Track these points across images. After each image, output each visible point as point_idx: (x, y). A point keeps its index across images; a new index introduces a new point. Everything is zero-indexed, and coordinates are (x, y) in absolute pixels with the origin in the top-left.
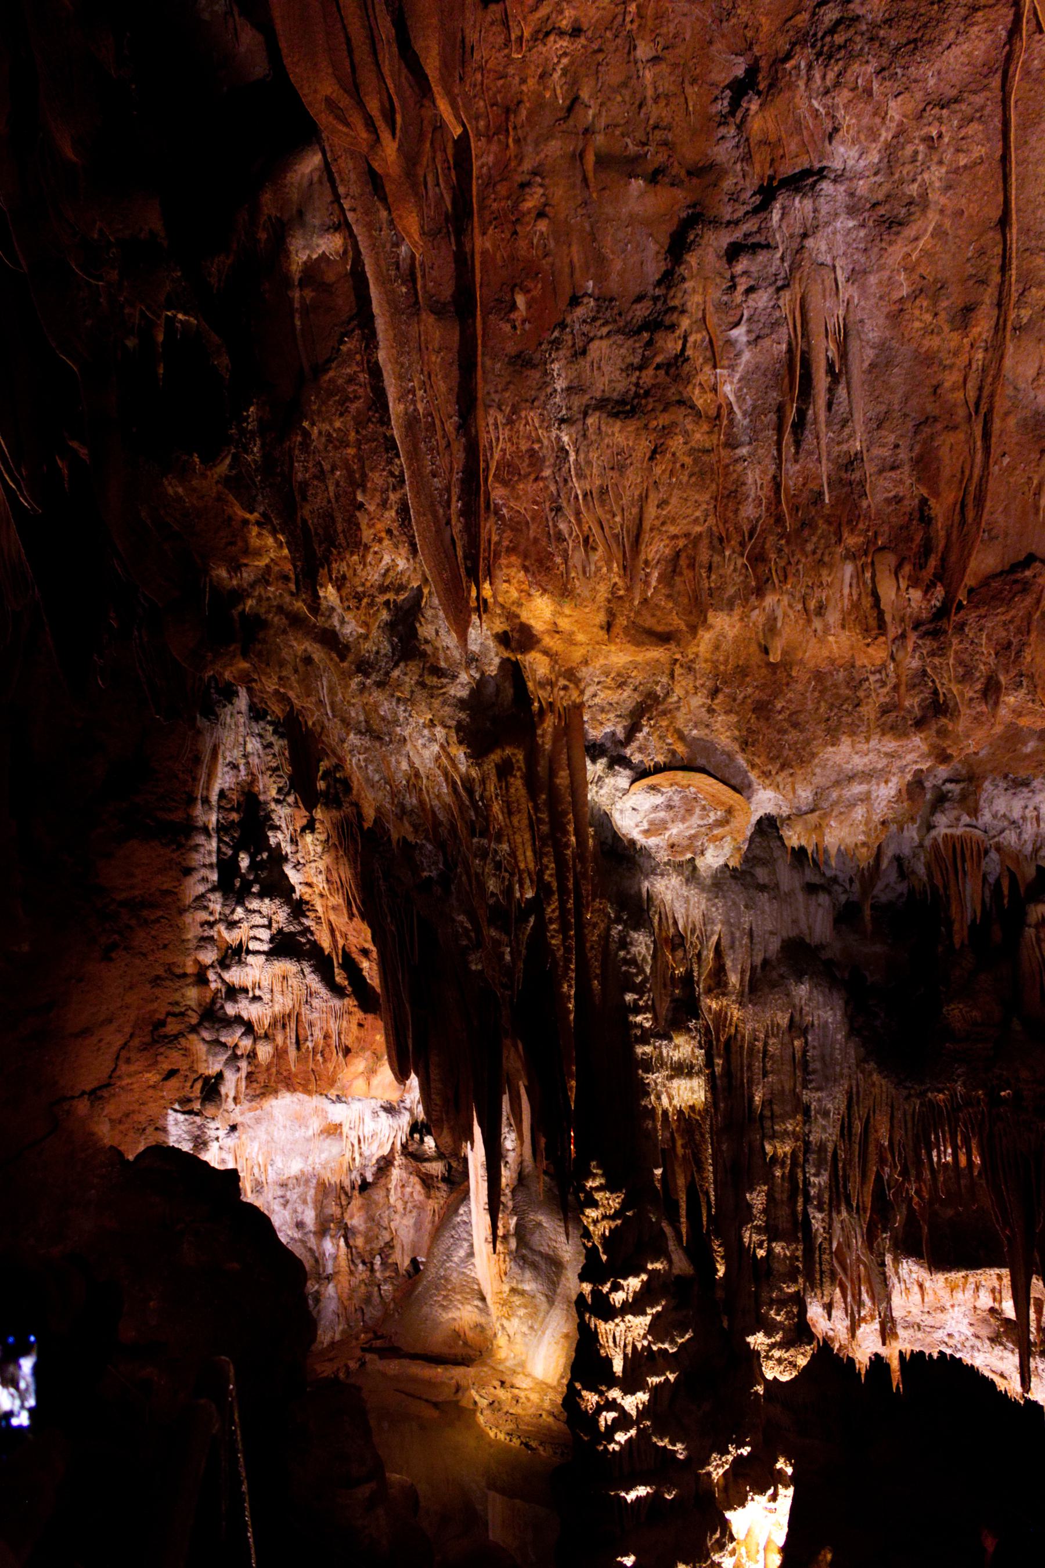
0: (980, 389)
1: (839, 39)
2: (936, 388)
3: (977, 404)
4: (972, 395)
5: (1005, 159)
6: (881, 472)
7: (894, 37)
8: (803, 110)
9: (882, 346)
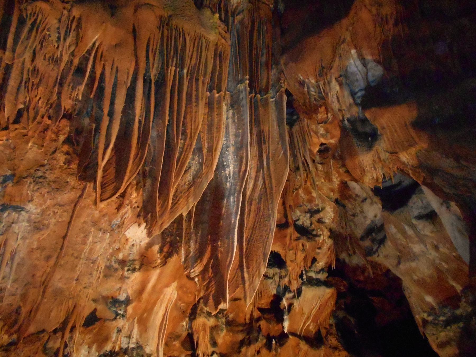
0: (46, 279)
1: (41, 180)
2: (33, 276)
3: (44, 283)
4: (43, 279)
5: (70, 223)
6: (9, 295)
7: (54, 186)
8: (24, 192)
9: (23, 259)
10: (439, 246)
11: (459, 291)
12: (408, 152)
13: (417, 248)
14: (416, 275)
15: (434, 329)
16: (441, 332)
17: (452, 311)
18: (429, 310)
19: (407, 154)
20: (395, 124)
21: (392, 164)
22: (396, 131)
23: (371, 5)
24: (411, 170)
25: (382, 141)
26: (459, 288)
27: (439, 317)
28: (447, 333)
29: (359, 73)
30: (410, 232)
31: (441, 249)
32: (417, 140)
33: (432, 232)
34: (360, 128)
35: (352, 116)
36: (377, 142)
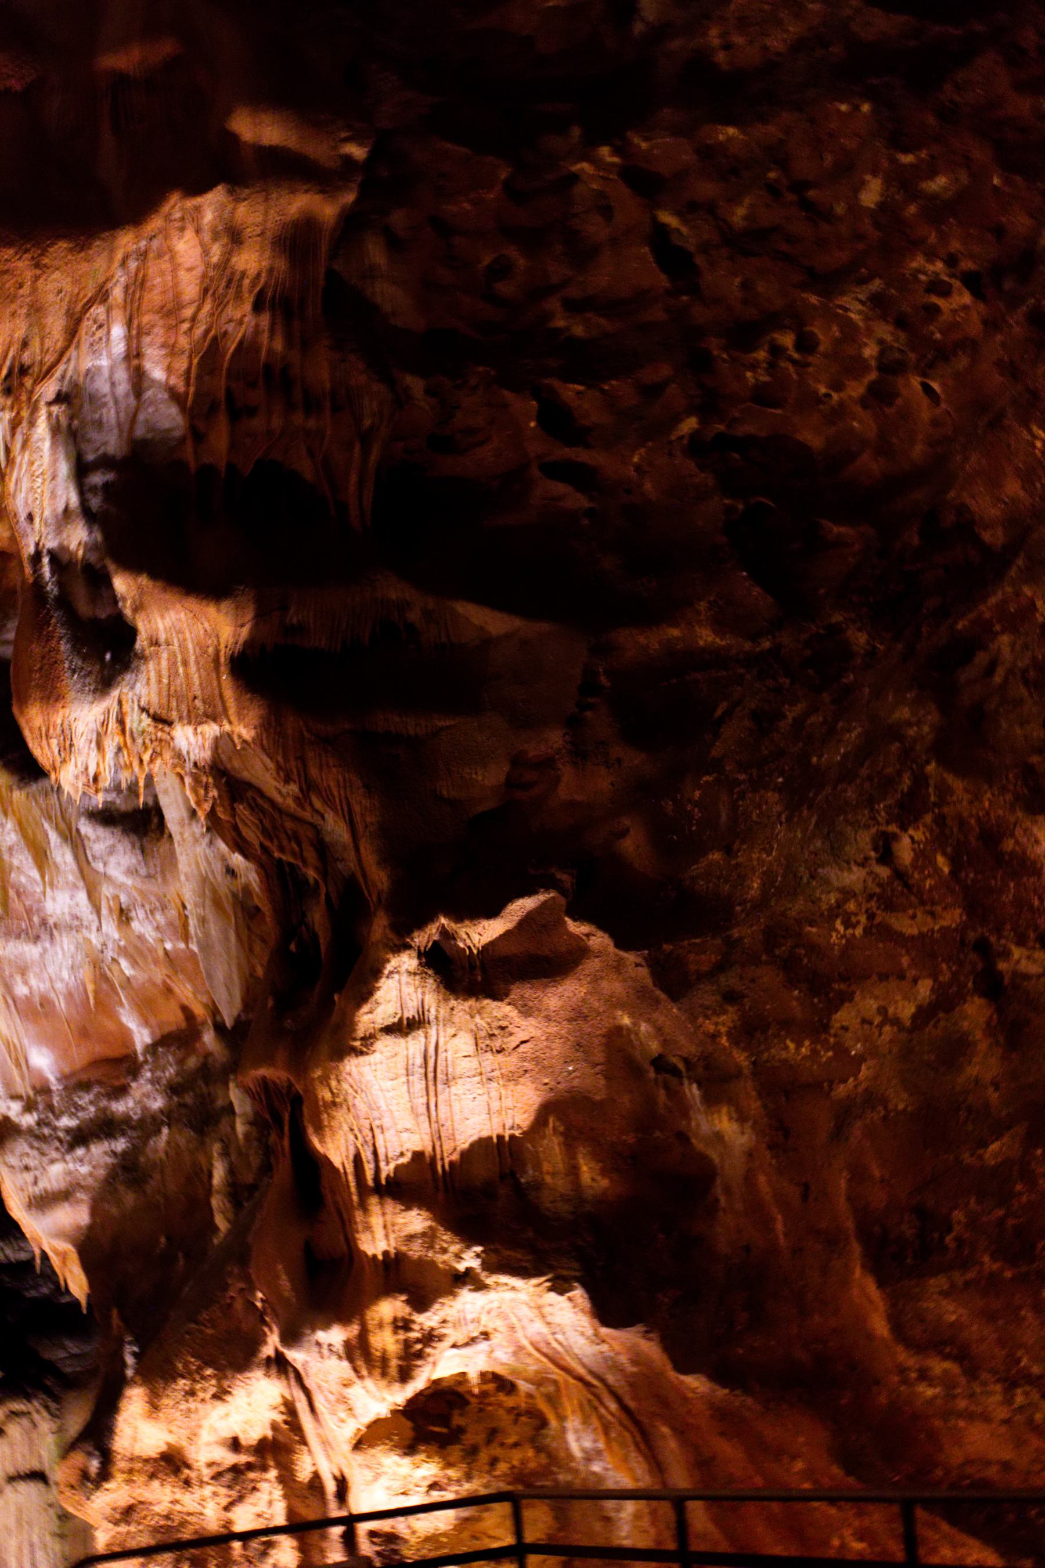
10: (133, 914)
11: (139, 1048)
12: (199, 730)
13: (63, 901)
14: (26, 983)
15: (35, 1153)
16: (53, 1161)
17: (104, 1103)
18: (31, 1093)
19: (195, 733)
20: (190, 646)
21: (150, 752)
22: (185, 663)
23: (216, 237)
24: (192, 774)
25: (142, 677)
26: (141, 1037)
27: (58, 1117)
28: (71, 1166)
29: (111, 404)
30: (62, 856)
31: (135, 925)
32: (232, 711)
33: (131, 872)
34: (84, 608)
35: (63, 548)
36: (128, 677)
